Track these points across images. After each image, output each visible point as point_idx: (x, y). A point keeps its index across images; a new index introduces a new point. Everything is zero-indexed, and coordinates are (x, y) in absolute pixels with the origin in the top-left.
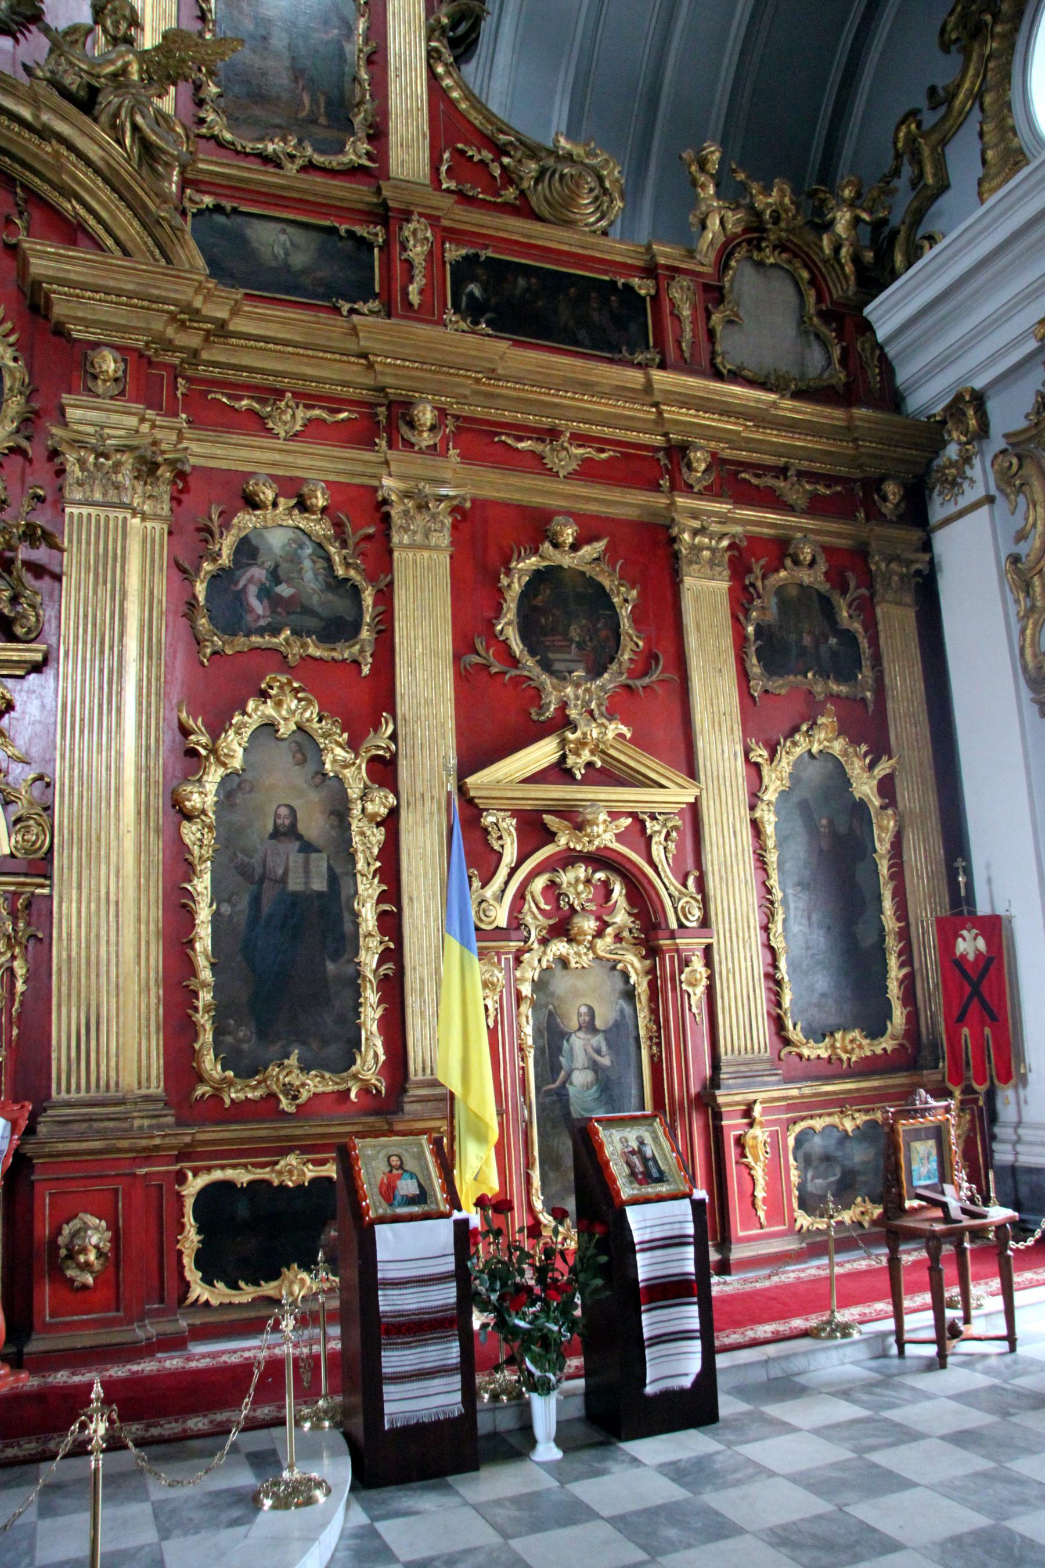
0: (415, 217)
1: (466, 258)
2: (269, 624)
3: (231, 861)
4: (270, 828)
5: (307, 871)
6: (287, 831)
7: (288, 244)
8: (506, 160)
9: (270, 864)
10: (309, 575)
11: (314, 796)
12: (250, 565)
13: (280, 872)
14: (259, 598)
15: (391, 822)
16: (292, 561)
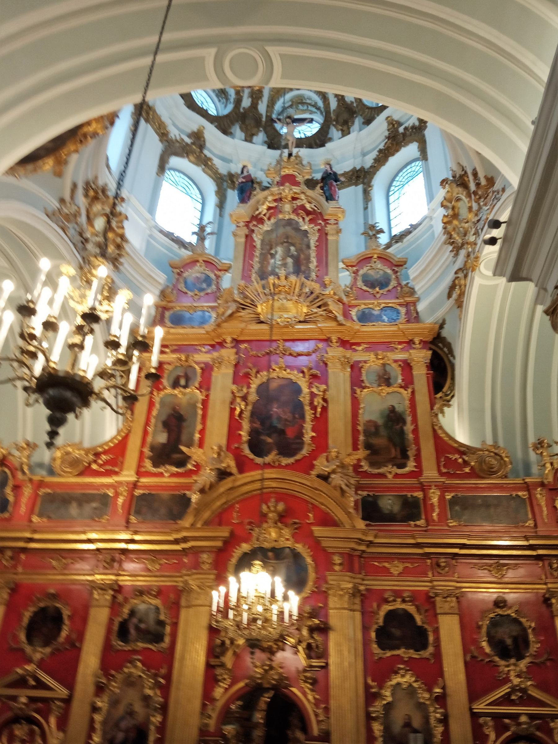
0: (433, 487)
8: (464, 457)
15: (445, 720)
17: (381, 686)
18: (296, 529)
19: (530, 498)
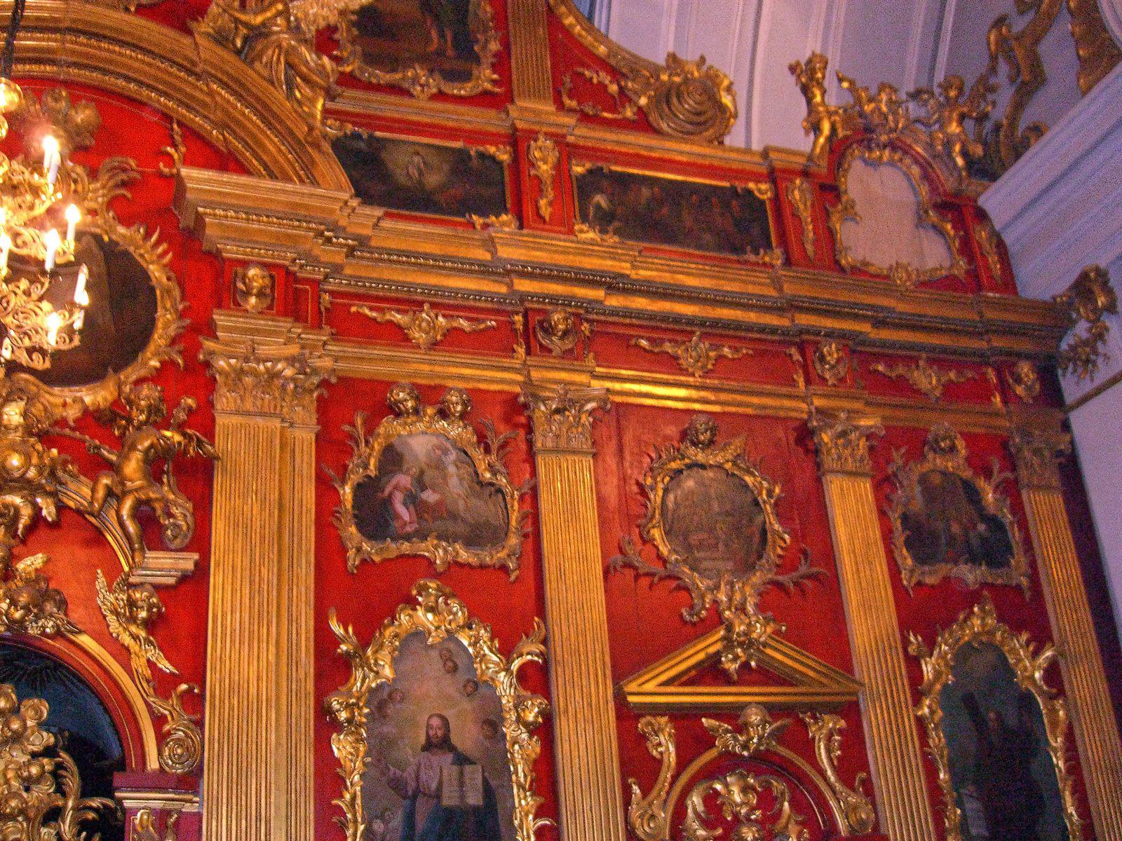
1: (590, 172)
3: (383, 774)
4: (422, 739)
5: (461, 784)
6: (440, 743)
9: (423, 777)
10: (453, 481)
11: (466, 705)
13: (434, 785)
14: (405, 504)
15: (545, 730)
16: (437, 468)
17: (365, 639)
18: (124, 184)
19: (776, 200)
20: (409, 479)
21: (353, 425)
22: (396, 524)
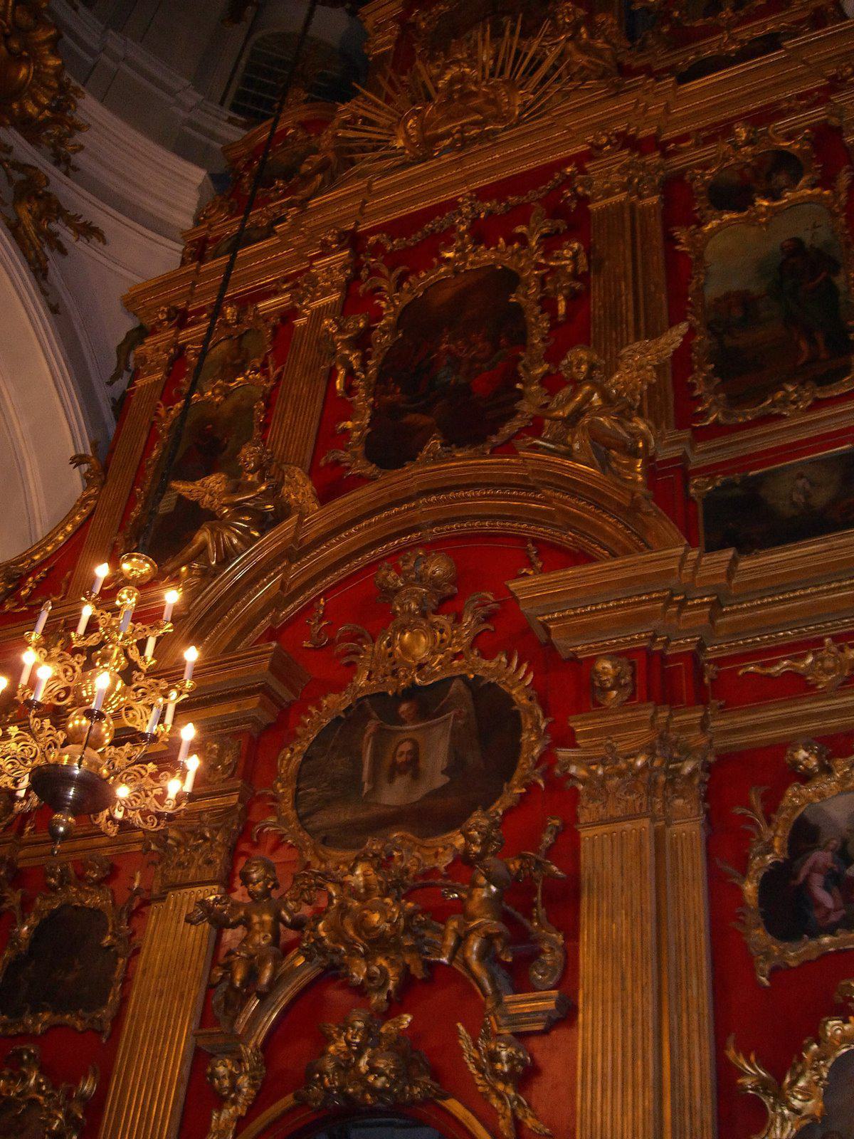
2: (844, 917)
7: (808, 487)
12: (812, 849)
14: (826, 887)
20: (829, 854)
21: (748, 805)
22: (816, 914)
